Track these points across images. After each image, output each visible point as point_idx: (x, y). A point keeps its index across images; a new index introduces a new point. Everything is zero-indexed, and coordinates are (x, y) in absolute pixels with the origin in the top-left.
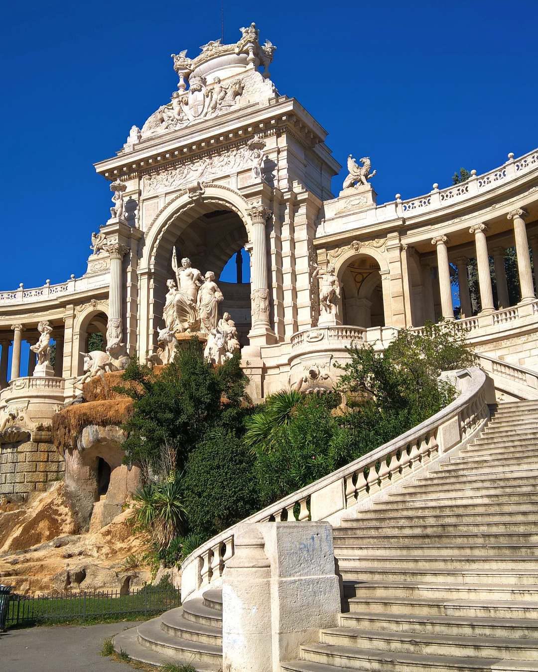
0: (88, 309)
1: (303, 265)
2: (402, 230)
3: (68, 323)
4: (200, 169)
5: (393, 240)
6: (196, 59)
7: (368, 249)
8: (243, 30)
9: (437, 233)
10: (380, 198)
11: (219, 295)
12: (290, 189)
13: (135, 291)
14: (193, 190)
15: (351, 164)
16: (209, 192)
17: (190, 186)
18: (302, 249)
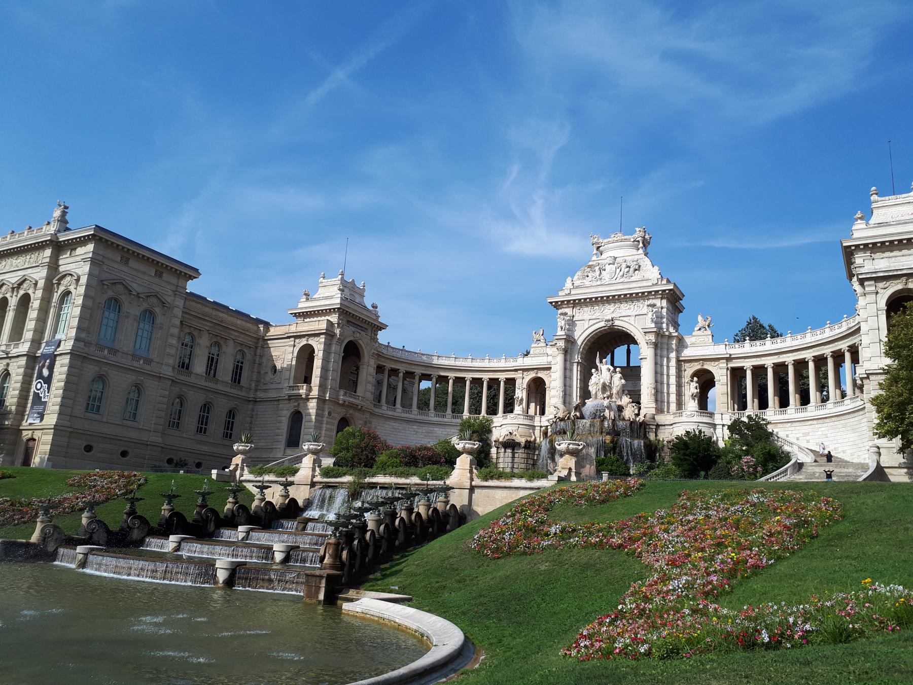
0: (532, 375)
1: (673, 371)
2: (729, 359)
3: (518, 382)
4: (612, 309)
5: (723, 364)
6: (606, 241)
7: (708, 366)
8: (638, 229)
9: (748, 364)
10: (716, 339)
11: (623, 381)
12: (668, 330)
13: (571, 370)
14: (608, 321)
15: (700, 318)
16: (617, 323)
17: (607, 318)
18: (673, 363)
